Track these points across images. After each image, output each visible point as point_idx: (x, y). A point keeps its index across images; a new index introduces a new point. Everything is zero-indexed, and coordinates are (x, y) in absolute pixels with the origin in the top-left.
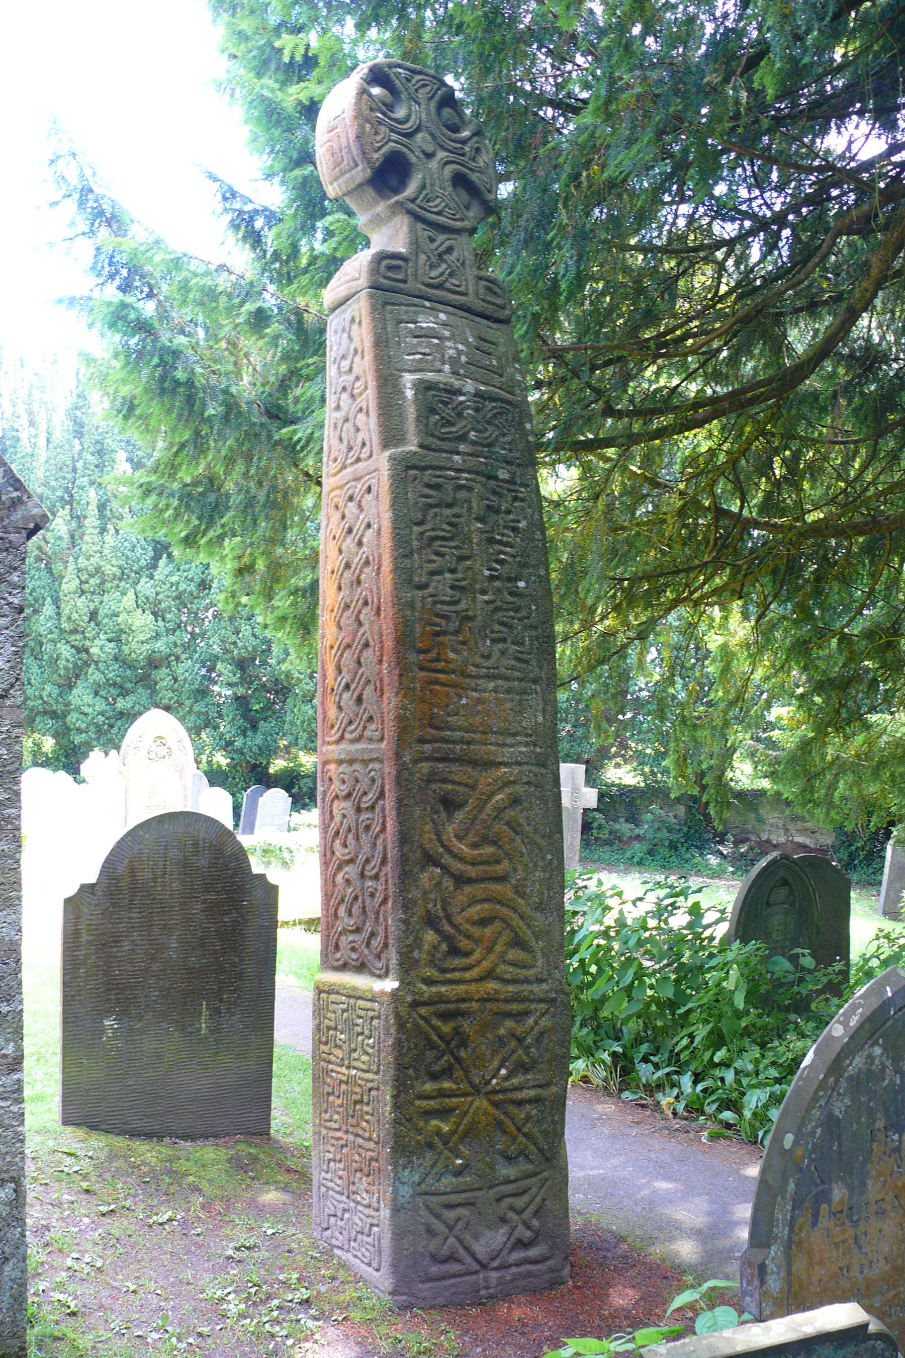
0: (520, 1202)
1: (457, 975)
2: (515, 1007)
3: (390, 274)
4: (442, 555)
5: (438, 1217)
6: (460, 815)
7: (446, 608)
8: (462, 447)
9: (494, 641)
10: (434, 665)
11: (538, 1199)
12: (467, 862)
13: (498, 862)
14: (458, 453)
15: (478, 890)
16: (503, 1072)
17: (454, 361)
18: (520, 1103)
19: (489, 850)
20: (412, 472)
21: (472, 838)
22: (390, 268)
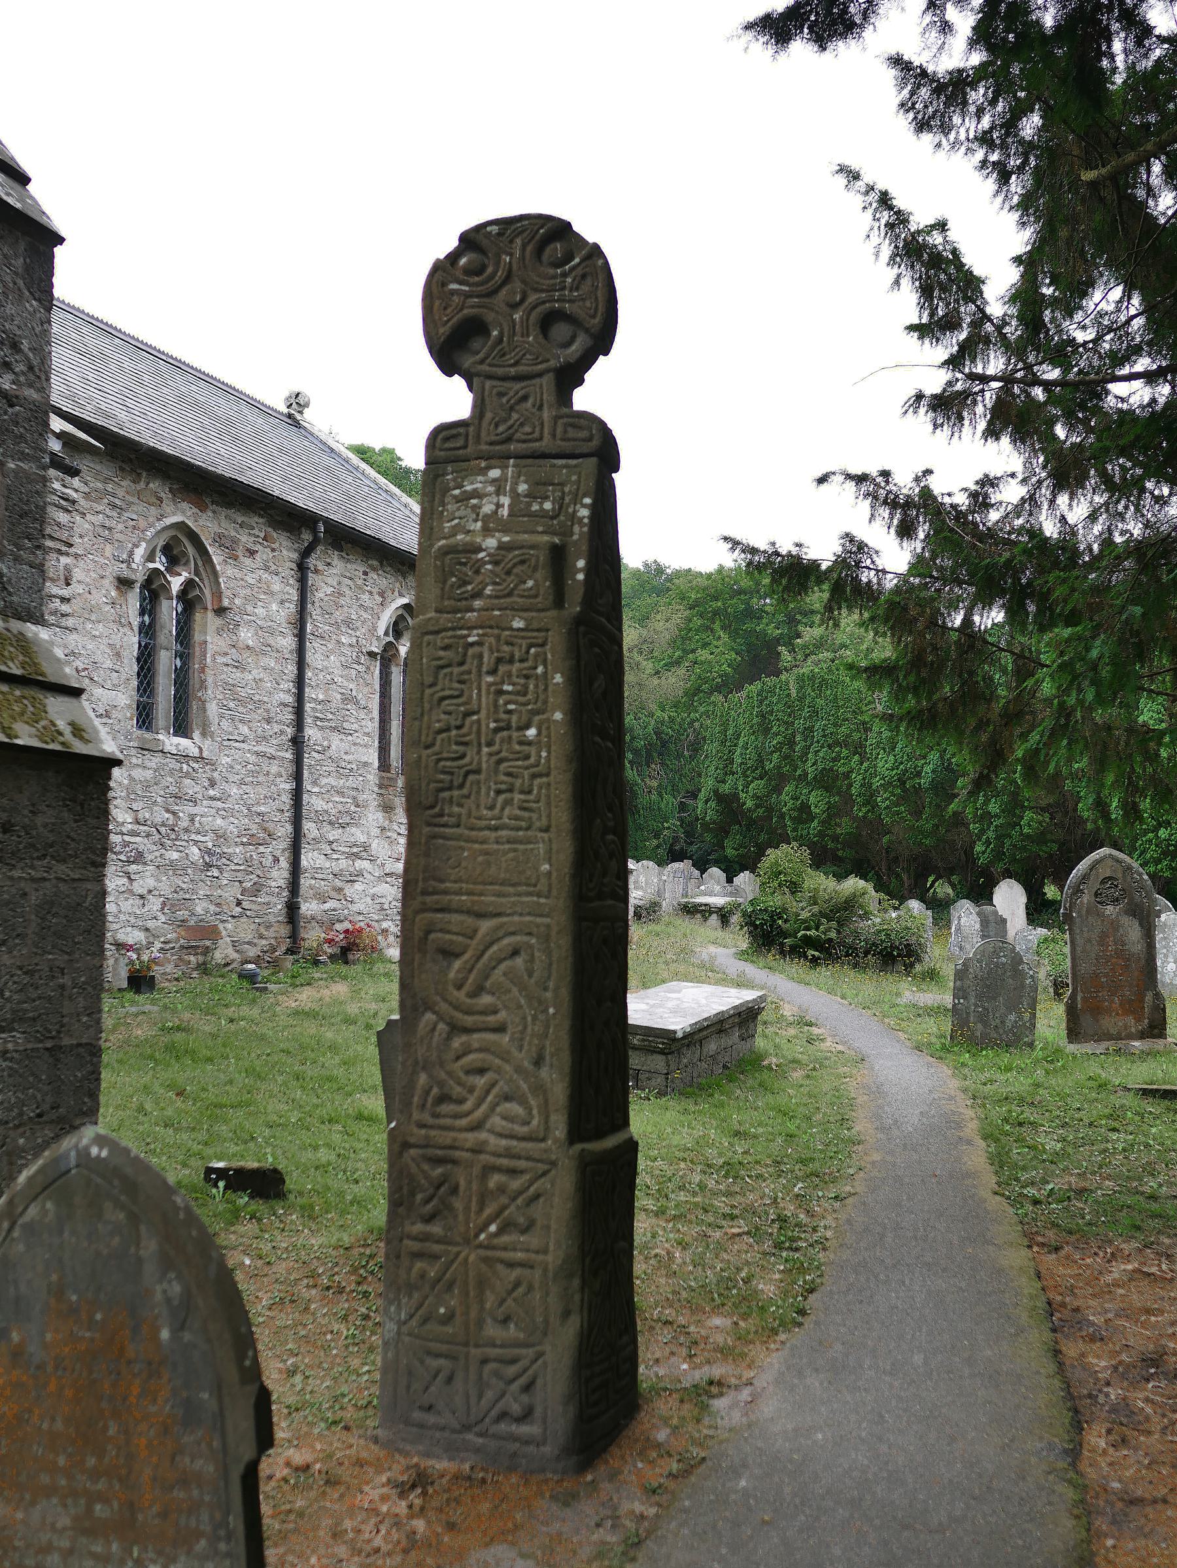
0: (512, 1370)
1: (448, 1121)
2: (505, 1162)
3: (447, 445)
4: (450, 713)
5: (422, 1362)
6: (457, 964)
7: (448, 763)
8: (477, 603)
9: (499, 792)
10: (437, 820)
11: (530, 1372)
12: (462, 1011)
13: (495, 1012)
14: (473, 610)
15: (476, 1039)
16: (493, 1228)
17: (486, 519)
18: (511, 1265)
19: (486, 999)
20: (427, 638)
21: (467, 987)
22: (447, 439)
